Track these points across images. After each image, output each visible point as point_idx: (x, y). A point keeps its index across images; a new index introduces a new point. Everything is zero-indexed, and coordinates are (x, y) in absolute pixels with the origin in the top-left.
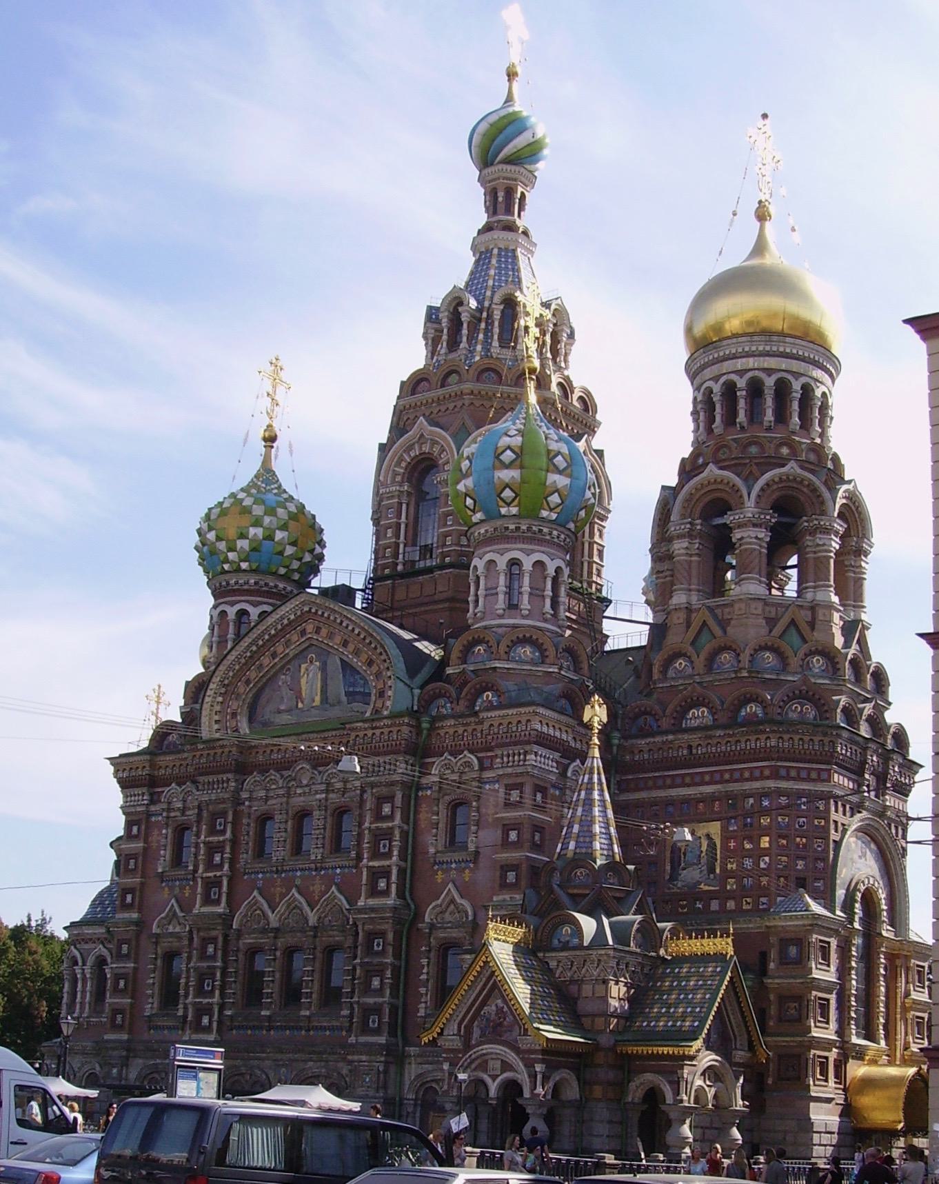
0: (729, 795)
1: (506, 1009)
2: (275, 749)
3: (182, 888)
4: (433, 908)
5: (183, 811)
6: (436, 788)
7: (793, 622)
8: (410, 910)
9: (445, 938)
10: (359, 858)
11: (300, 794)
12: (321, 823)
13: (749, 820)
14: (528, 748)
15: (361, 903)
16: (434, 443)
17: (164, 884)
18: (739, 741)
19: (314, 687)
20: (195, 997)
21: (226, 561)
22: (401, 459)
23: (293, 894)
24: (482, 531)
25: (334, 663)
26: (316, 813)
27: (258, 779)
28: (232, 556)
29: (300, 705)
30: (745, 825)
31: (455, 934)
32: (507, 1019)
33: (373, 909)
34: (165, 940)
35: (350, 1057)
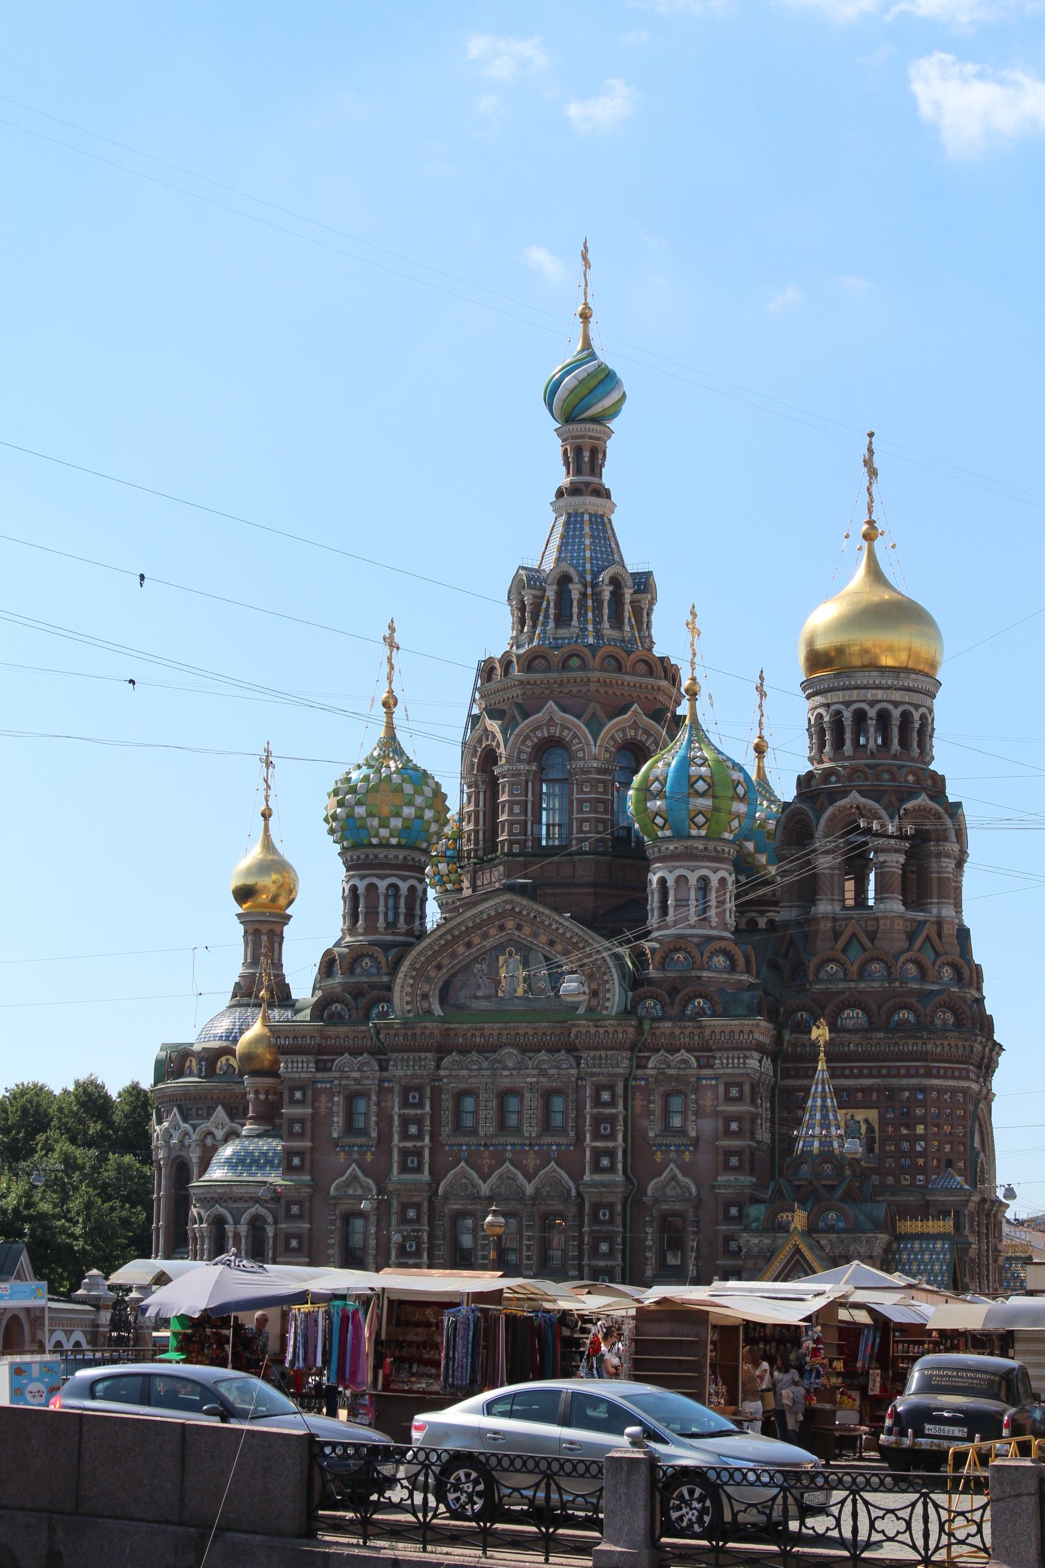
0: (886, 1088)
2: (478, 1033)
3: (362, 1154)
7: (928, 937)
10: (580, 1139)
11: (506, 1076)
12: (534, 1104)
14: (748, 1053)
15: (587, 1178)
16: (564, 727)
17: (338, 1149)
18: (897, 1043)
21: (377, 835)
22: (527, 737)
24: (671, 847)
26: (528, 1095)
28: (384, 832)
29: (500, 994)
30: (902, 1114)
31: (677, 1207)
33: (603, 1184)
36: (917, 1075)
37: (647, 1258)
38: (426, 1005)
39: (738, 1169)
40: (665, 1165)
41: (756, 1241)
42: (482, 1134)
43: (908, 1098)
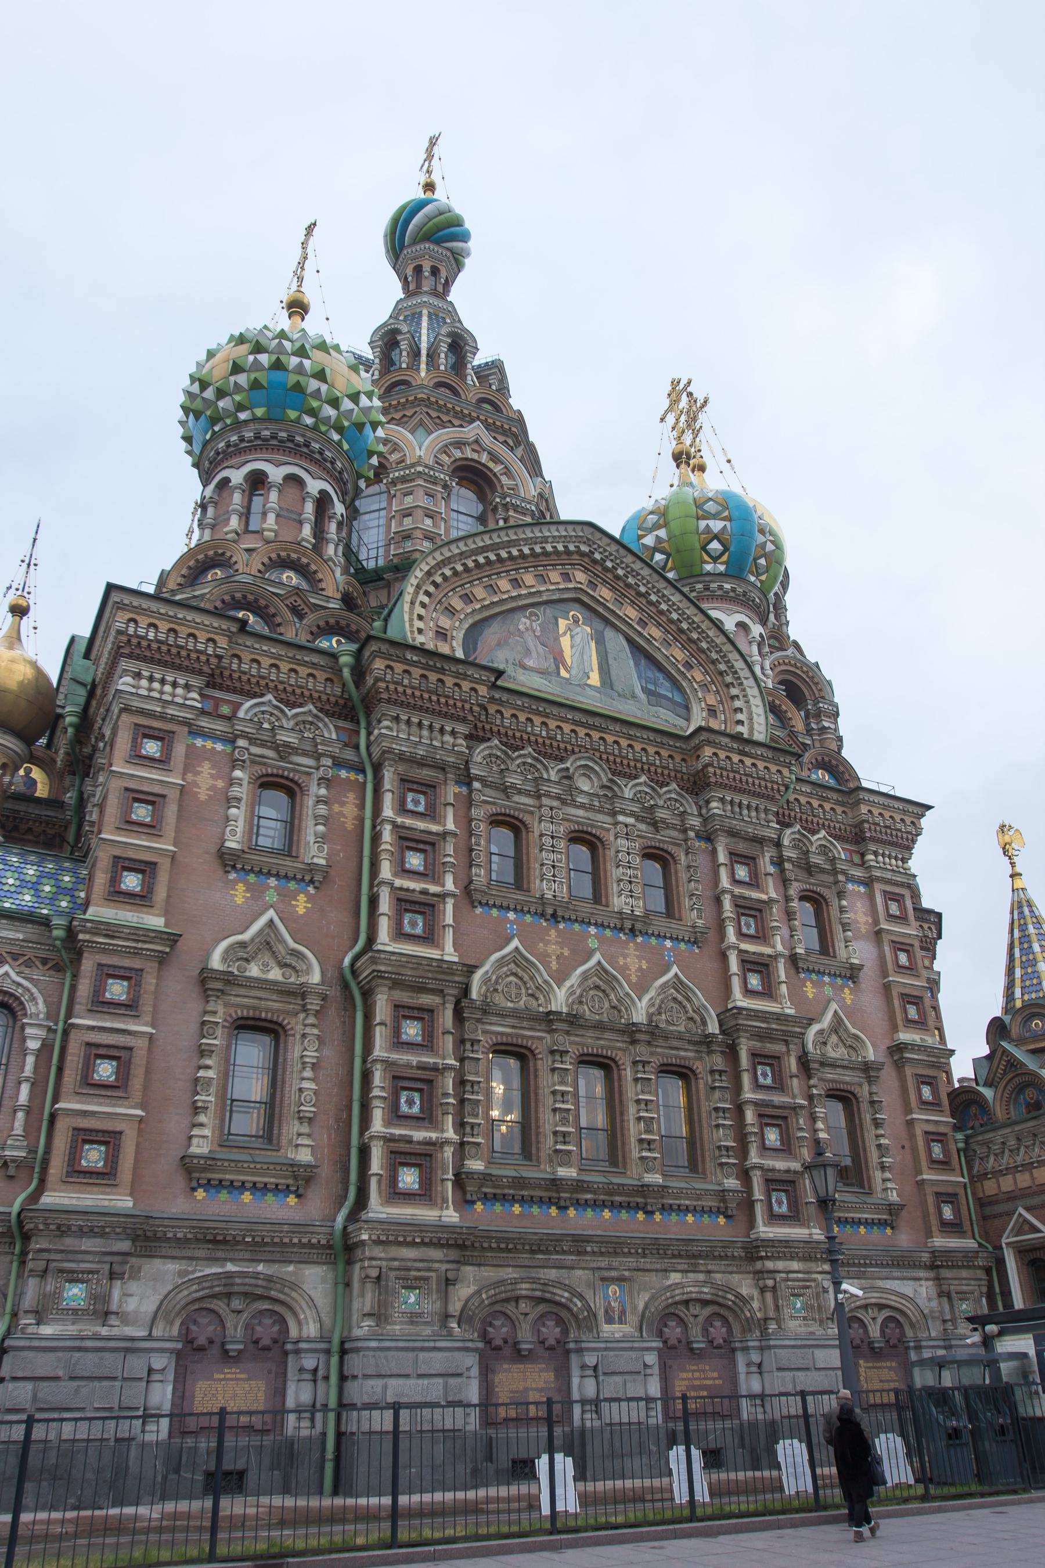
2: (537, 720)
5: (284, 751)
9: (835, 1081)
11: (582, 806)
16: (494, 458)
17: (232, 876)
19: (585, 657)
20: (388, 1123)
22: (445, 450)
23: (599, 962)
24: (727, 586)
25: (616, 642)
27: (499, 754)
28: (329, 411)
29: (563, 673)
34: (242, 991)
35: (770, 1265)
38: (444, 649)
42: (549, 895)
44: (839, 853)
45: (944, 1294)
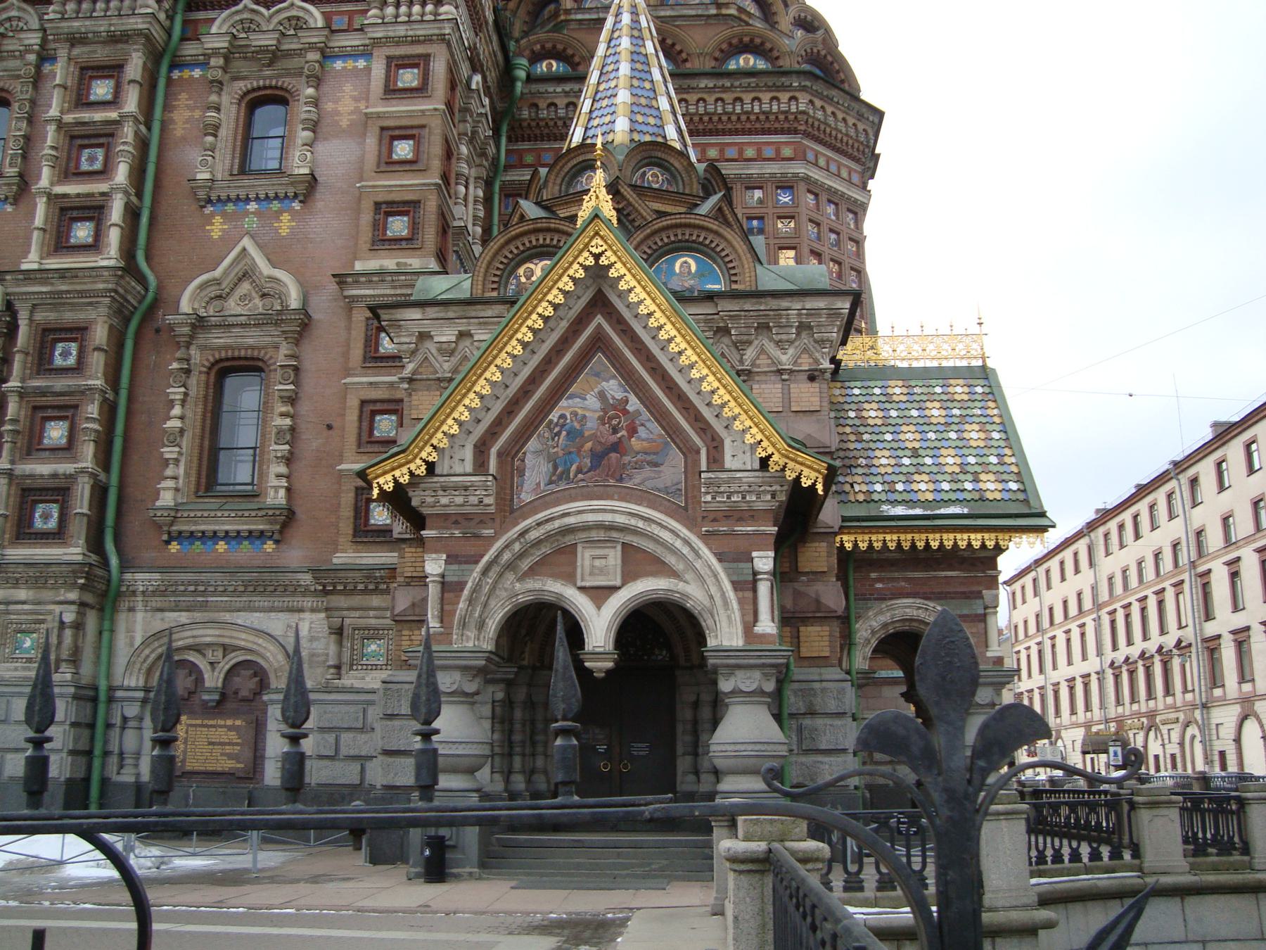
1: (634, 404)
4: (202, 287)
6: (217, 62)
8: (147, 290)
13: (755, 223)
18: (739, 99)
31: (251, 339)
32: (642, 432)
33: (63, 274)
36: (778, 158)
37: (166, 462)
39: (408, 243)
40: (229, 241)
41: (446, 335)
43: (760, 201)
44: (316, 21)
45: (339, 632)
